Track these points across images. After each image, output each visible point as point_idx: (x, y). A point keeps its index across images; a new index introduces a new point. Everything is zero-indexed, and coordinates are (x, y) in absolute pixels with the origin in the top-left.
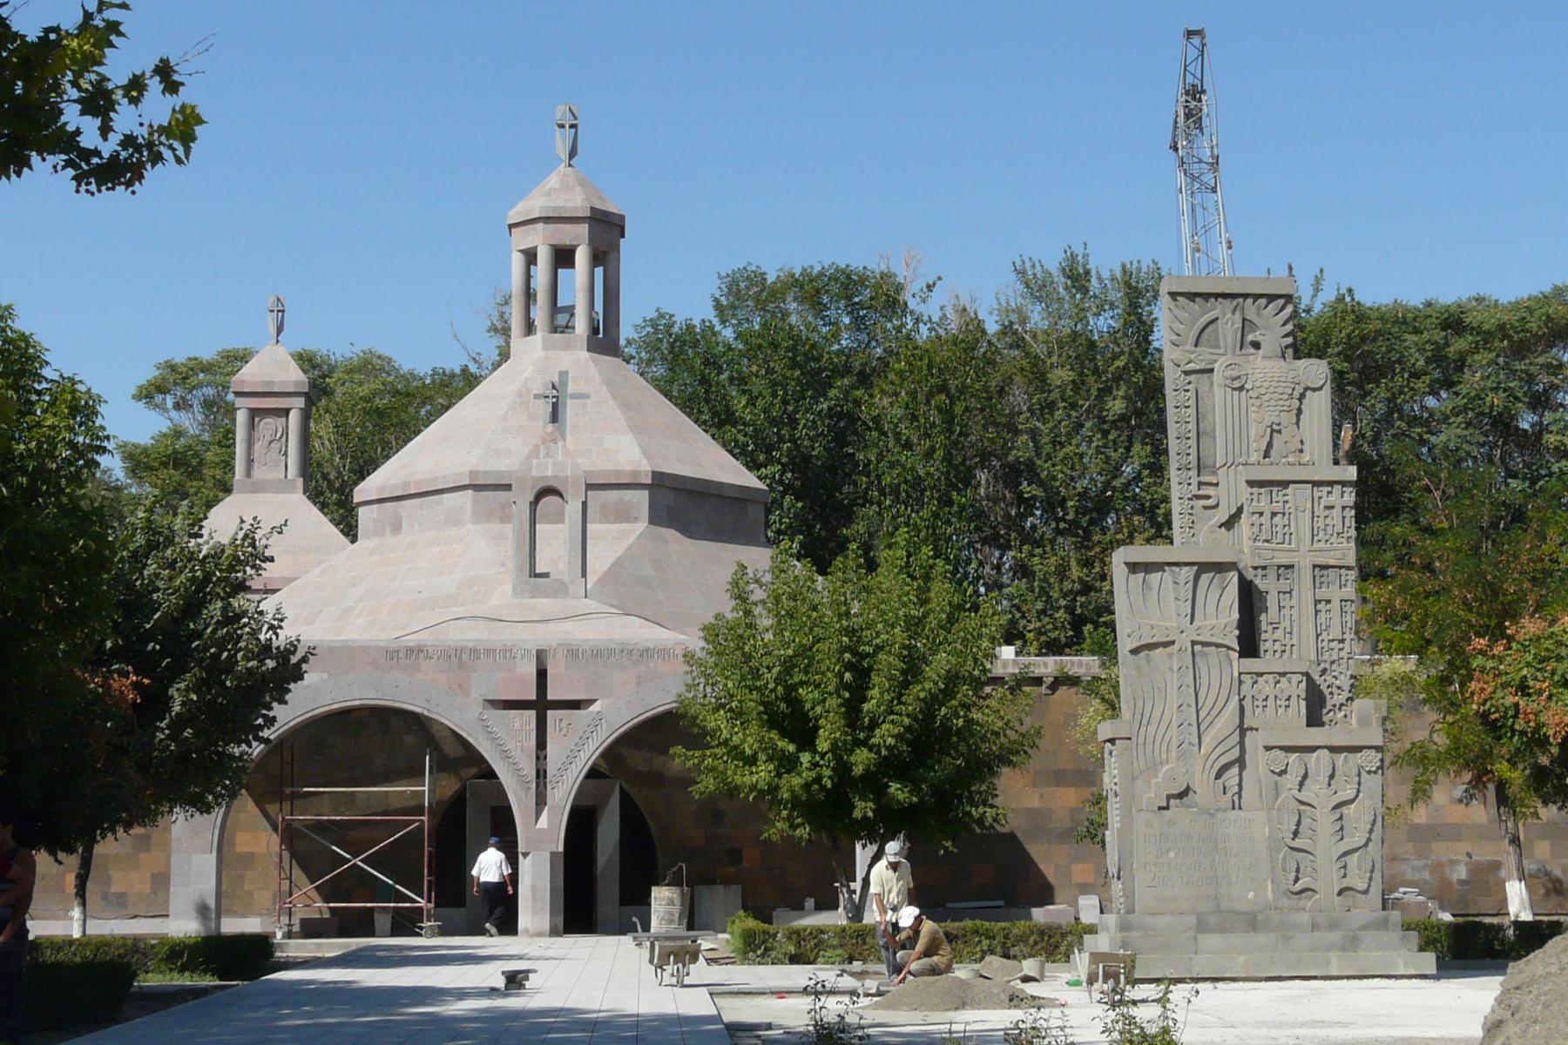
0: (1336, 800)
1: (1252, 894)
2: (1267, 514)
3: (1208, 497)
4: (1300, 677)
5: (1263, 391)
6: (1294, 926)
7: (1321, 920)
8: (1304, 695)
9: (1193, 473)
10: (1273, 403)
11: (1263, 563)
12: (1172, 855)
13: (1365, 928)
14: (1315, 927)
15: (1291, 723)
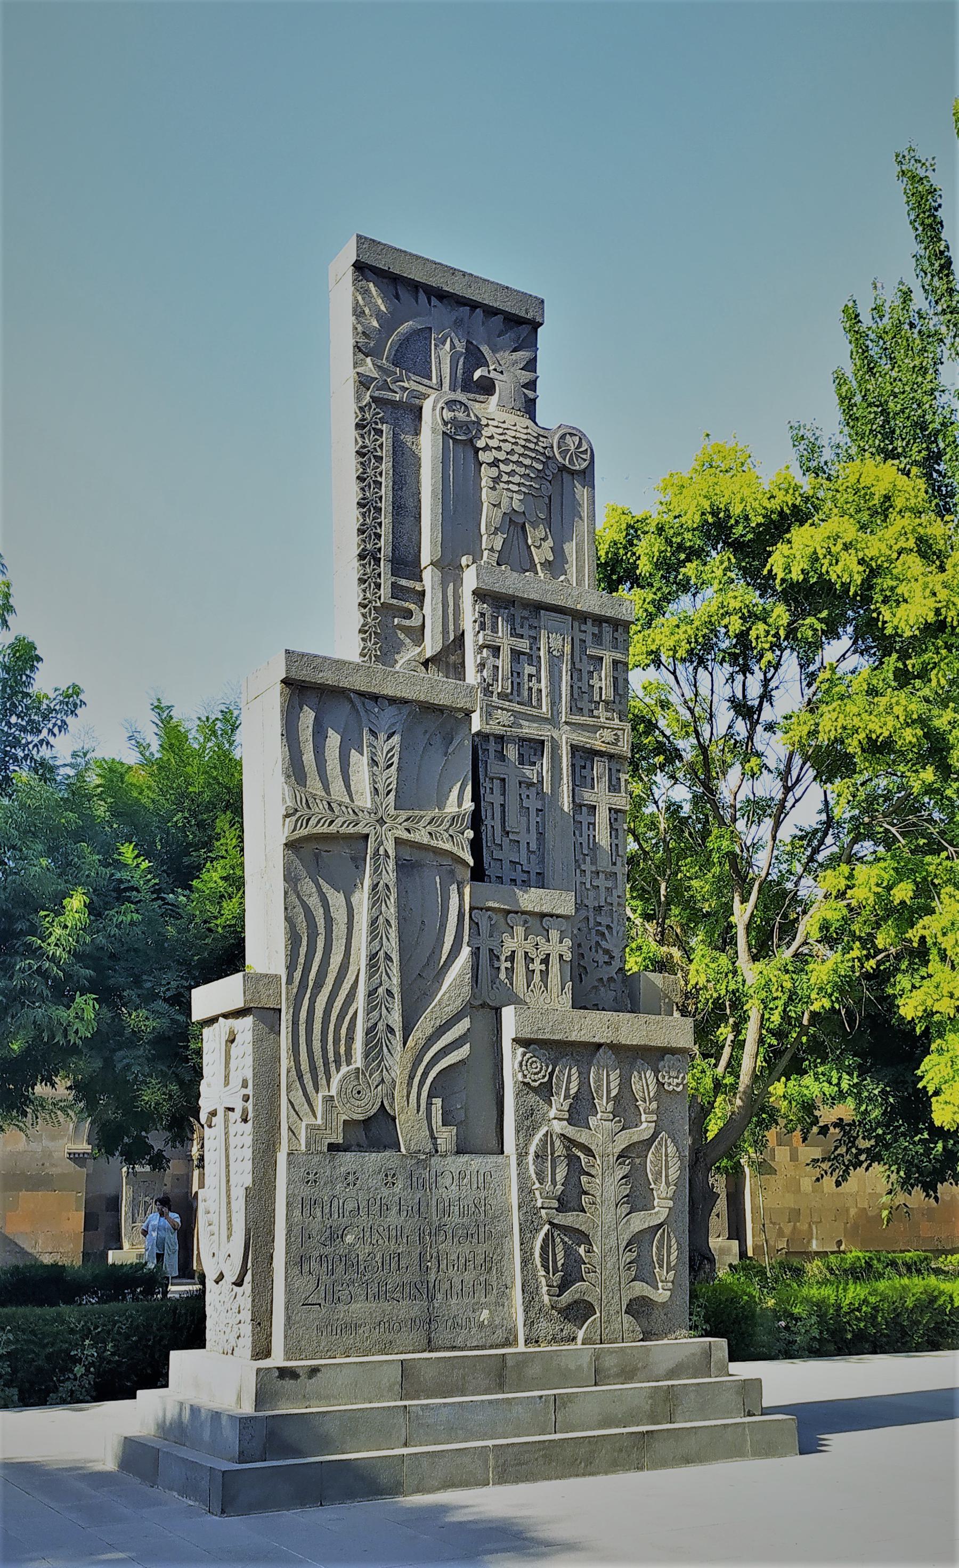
0: (623, 1141)
1: (485, 1314)
2: (505, 653)
3: (409, 614)
4: (564, 925)
5: (501, 456)
6: (566, 1377)
7: (610, 1362)
8: (568, 956)
9: (385, 568)
10: (517, 479)
11: (499, 730)
12: (349, 1239)
13: (672, 1373)
14: (599, 1376)
15: (541, 1006)
